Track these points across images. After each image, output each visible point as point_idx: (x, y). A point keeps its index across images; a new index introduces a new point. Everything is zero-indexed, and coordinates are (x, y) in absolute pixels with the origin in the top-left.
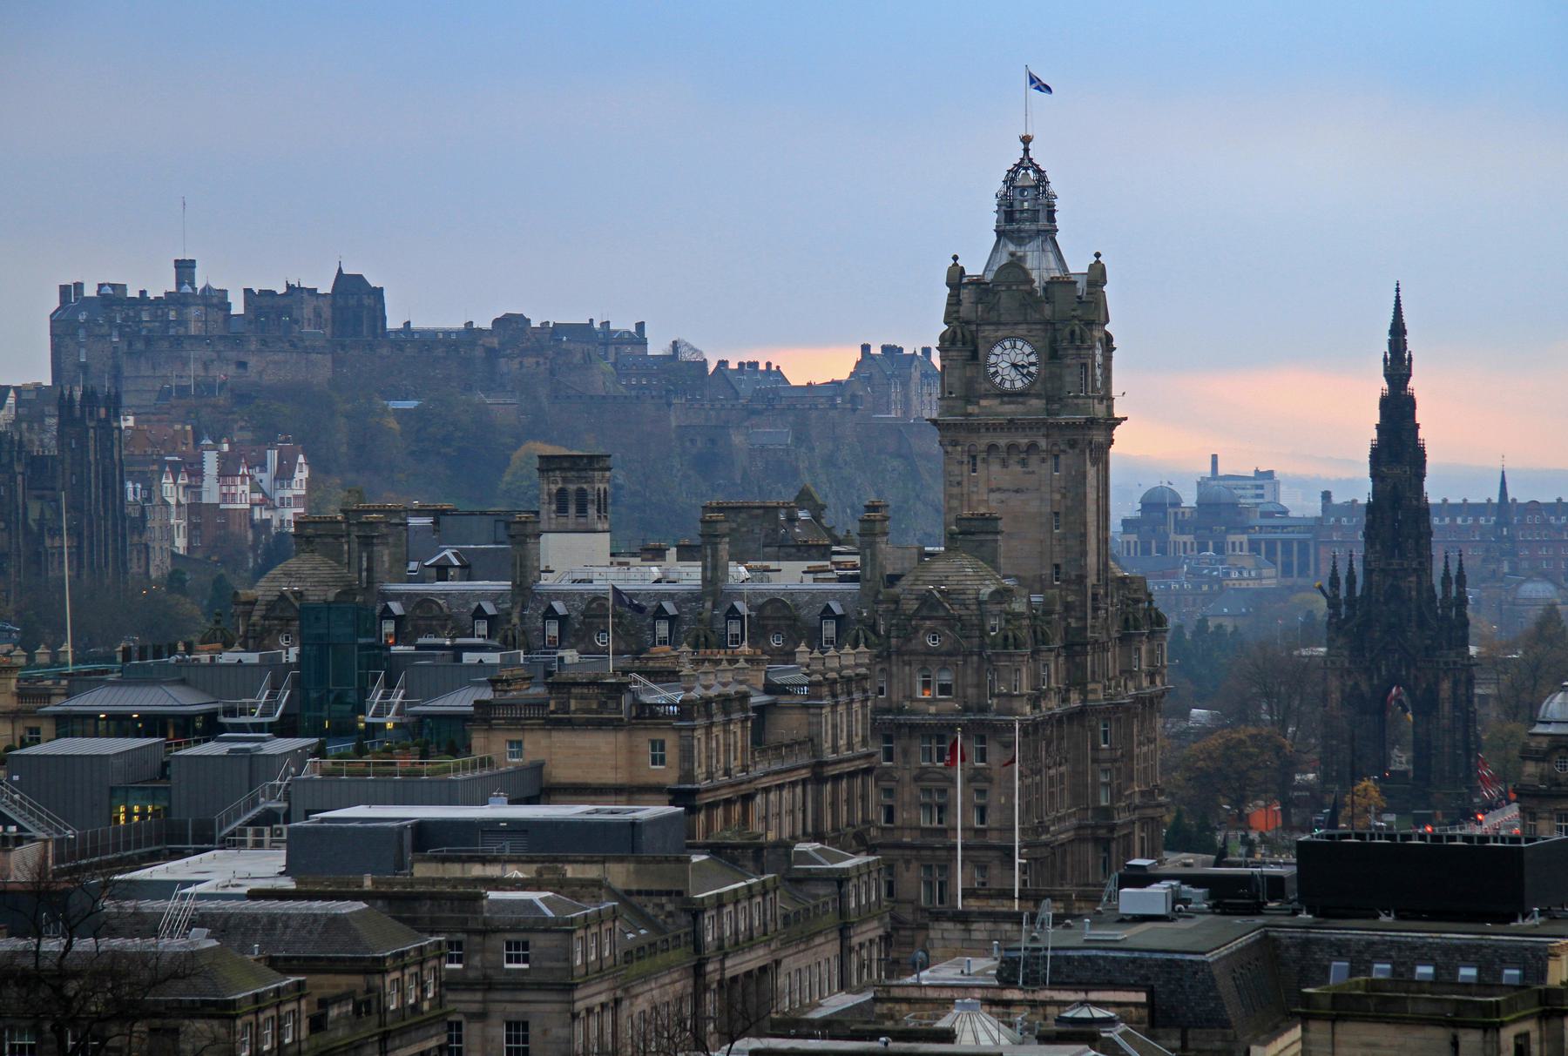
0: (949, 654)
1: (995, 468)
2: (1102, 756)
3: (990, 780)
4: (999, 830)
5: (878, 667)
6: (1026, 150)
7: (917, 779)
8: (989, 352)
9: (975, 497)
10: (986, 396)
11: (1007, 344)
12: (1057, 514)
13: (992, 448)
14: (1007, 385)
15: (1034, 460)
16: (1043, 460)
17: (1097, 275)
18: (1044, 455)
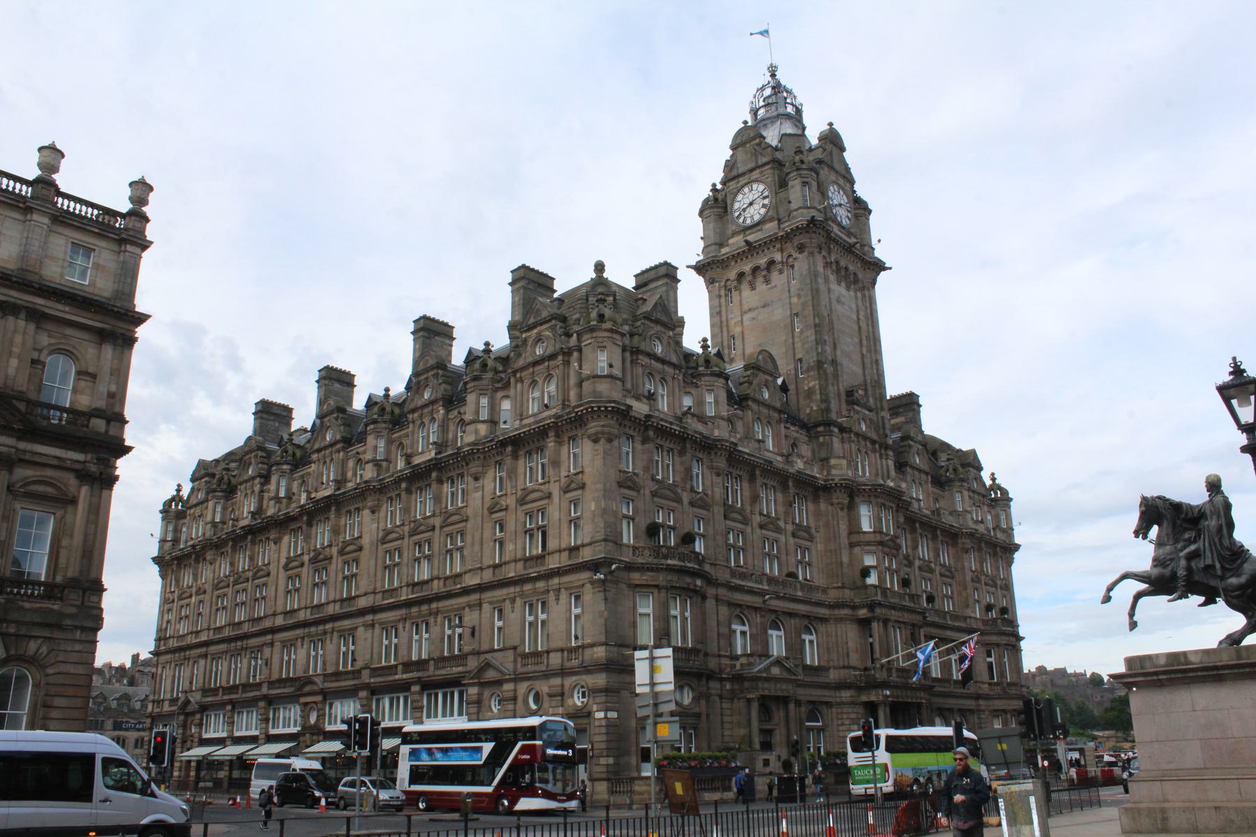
0: (552, 357)
1: (746, 292)
2: (862, 538)
3: (582, 487)
4: (590, 544)
5: (500, 394)
6: (773, 76)
7: (522, 502)
8: (734, 200)
9: (732, 323)
10: (733, 235)
11: (746, 190)
12: (797, 315)
13: (741, 275)
14: (749, 221)
15: (775, 276)
16: (781, 272)
17: (832, 140)
18: (779, 266)
